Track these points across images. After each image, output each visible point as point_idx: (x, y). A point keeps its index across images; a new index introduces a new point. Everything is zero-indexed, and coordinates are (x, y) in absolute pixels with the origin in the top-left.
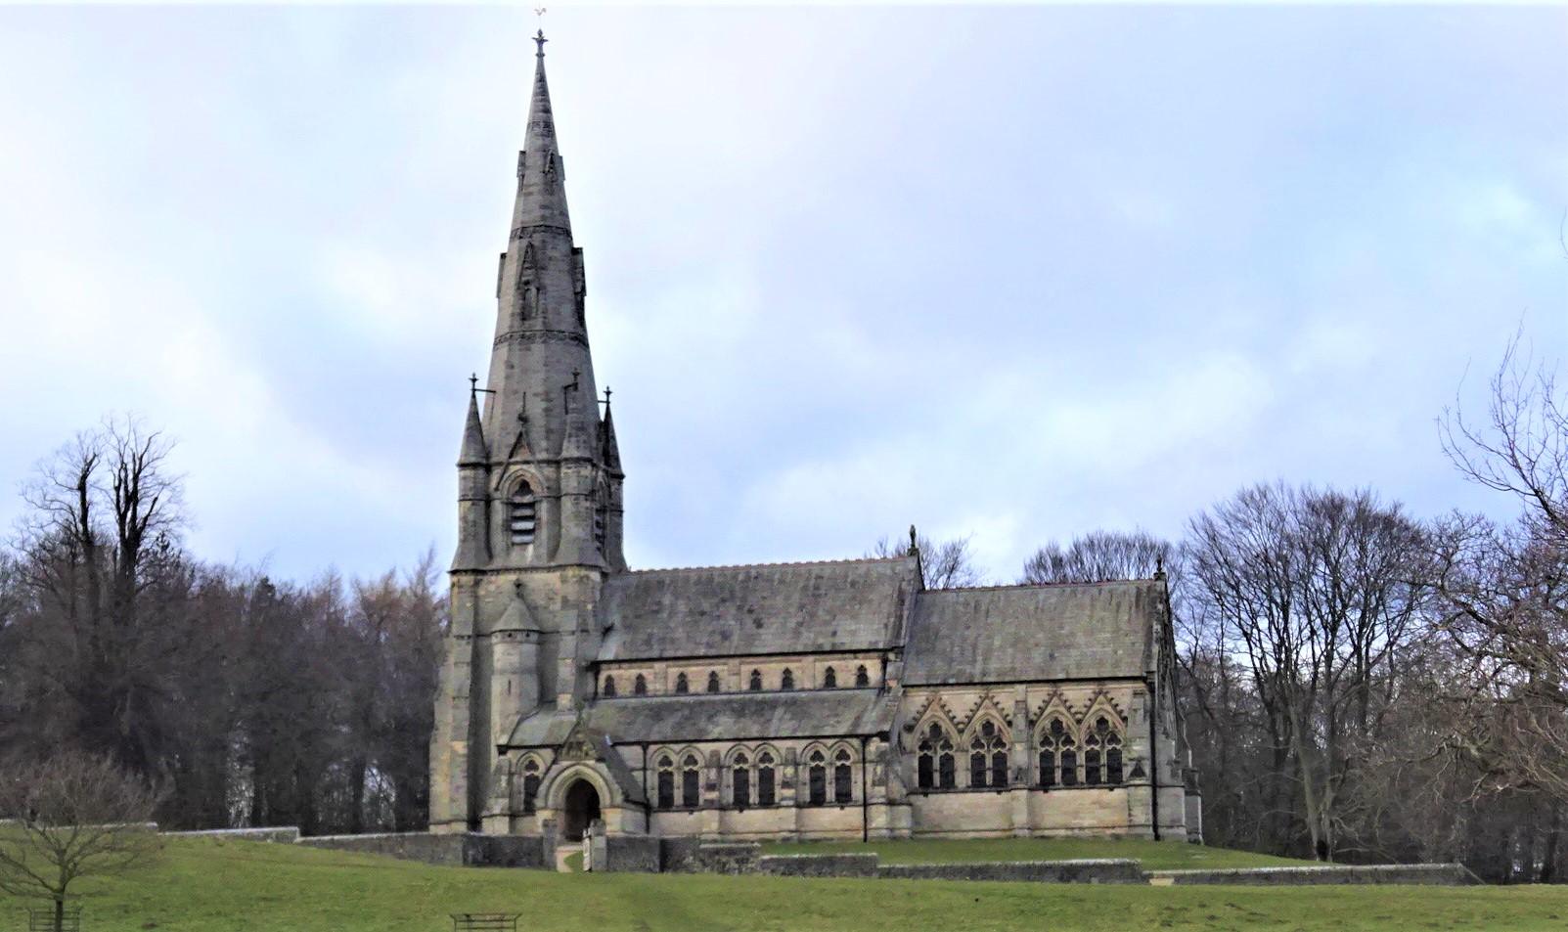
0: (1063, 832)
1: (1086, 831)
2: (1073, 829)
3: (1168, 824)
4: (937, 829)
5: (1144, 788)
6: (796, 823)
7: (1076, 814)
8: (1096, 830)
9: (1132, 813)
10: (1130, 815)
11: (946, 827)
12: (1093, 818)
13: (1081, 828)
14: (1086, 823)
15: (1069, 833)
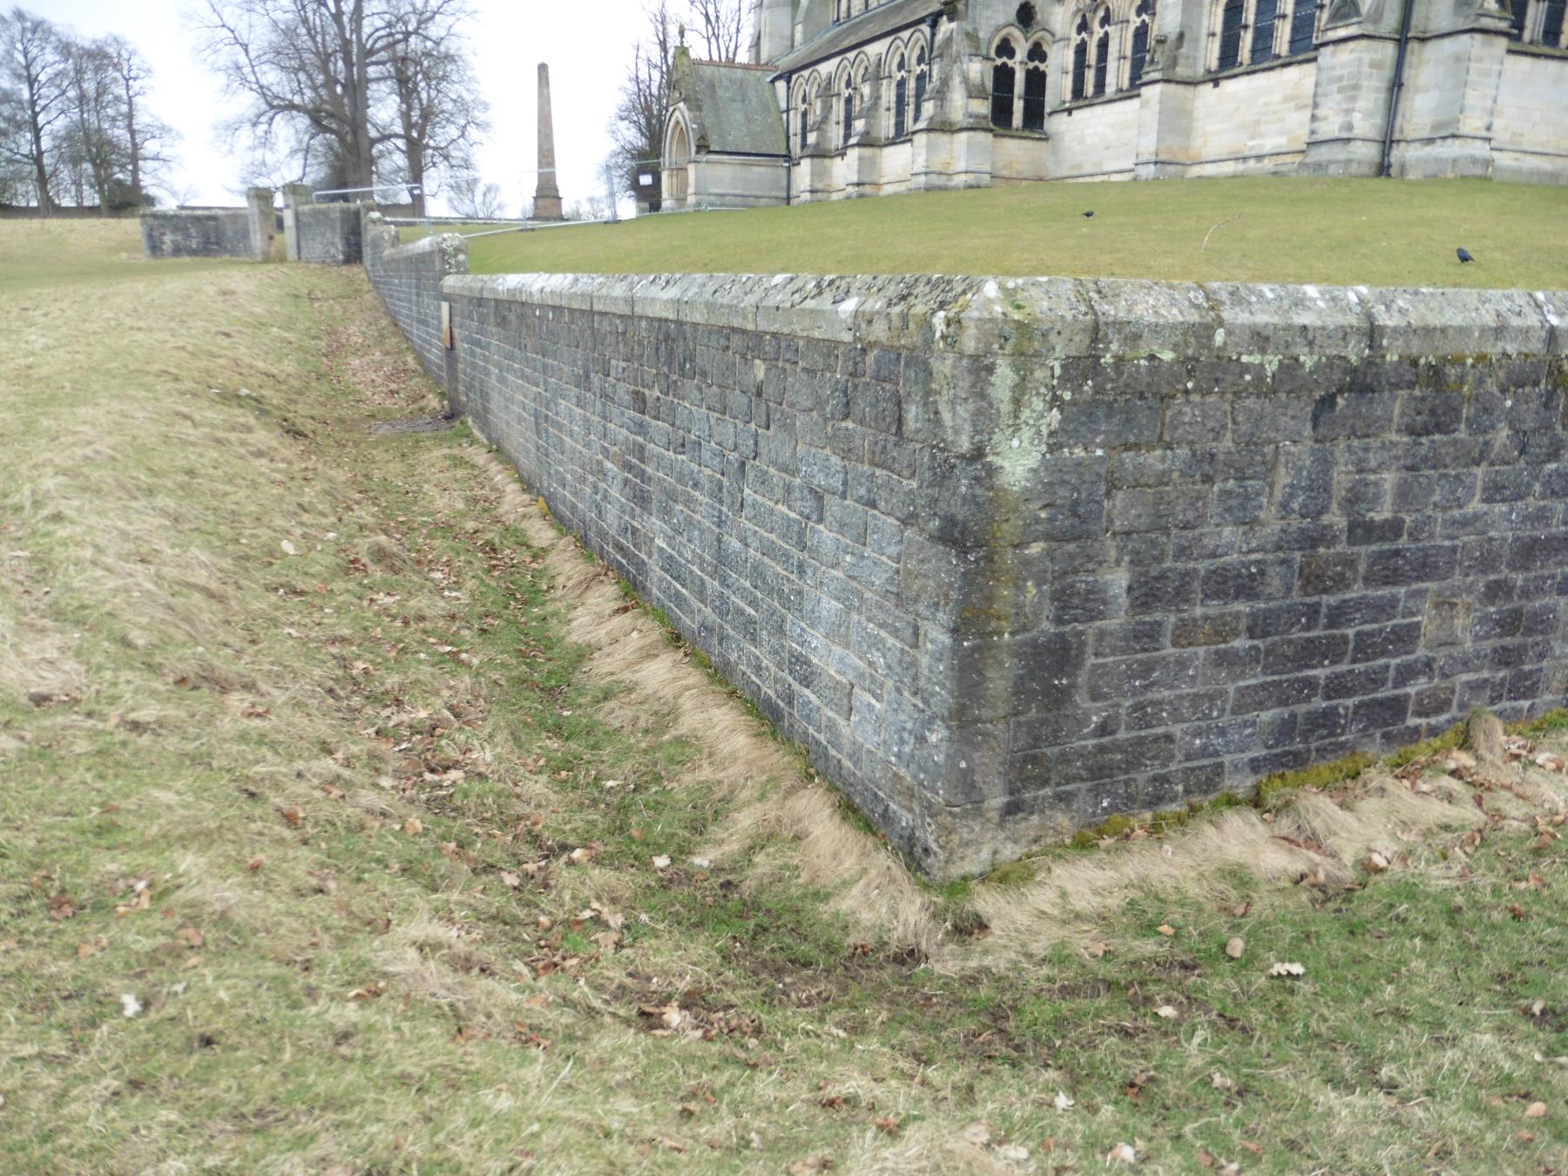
0: (1229, 168)
1: (1266, 161)
2: (1245, 159)
3: (1426, 134)
4: (1076, 172)
5: (1351, 45)
6: (859, 172)
7: (1254, 129)
8: (1281, 159)
9: (1320, 112)
10: (1314, 118)
11: (1088, 169)
12: (1281, 133)
13: (1259, 158)
14: (1269, 144)
15: (1240, 167)
